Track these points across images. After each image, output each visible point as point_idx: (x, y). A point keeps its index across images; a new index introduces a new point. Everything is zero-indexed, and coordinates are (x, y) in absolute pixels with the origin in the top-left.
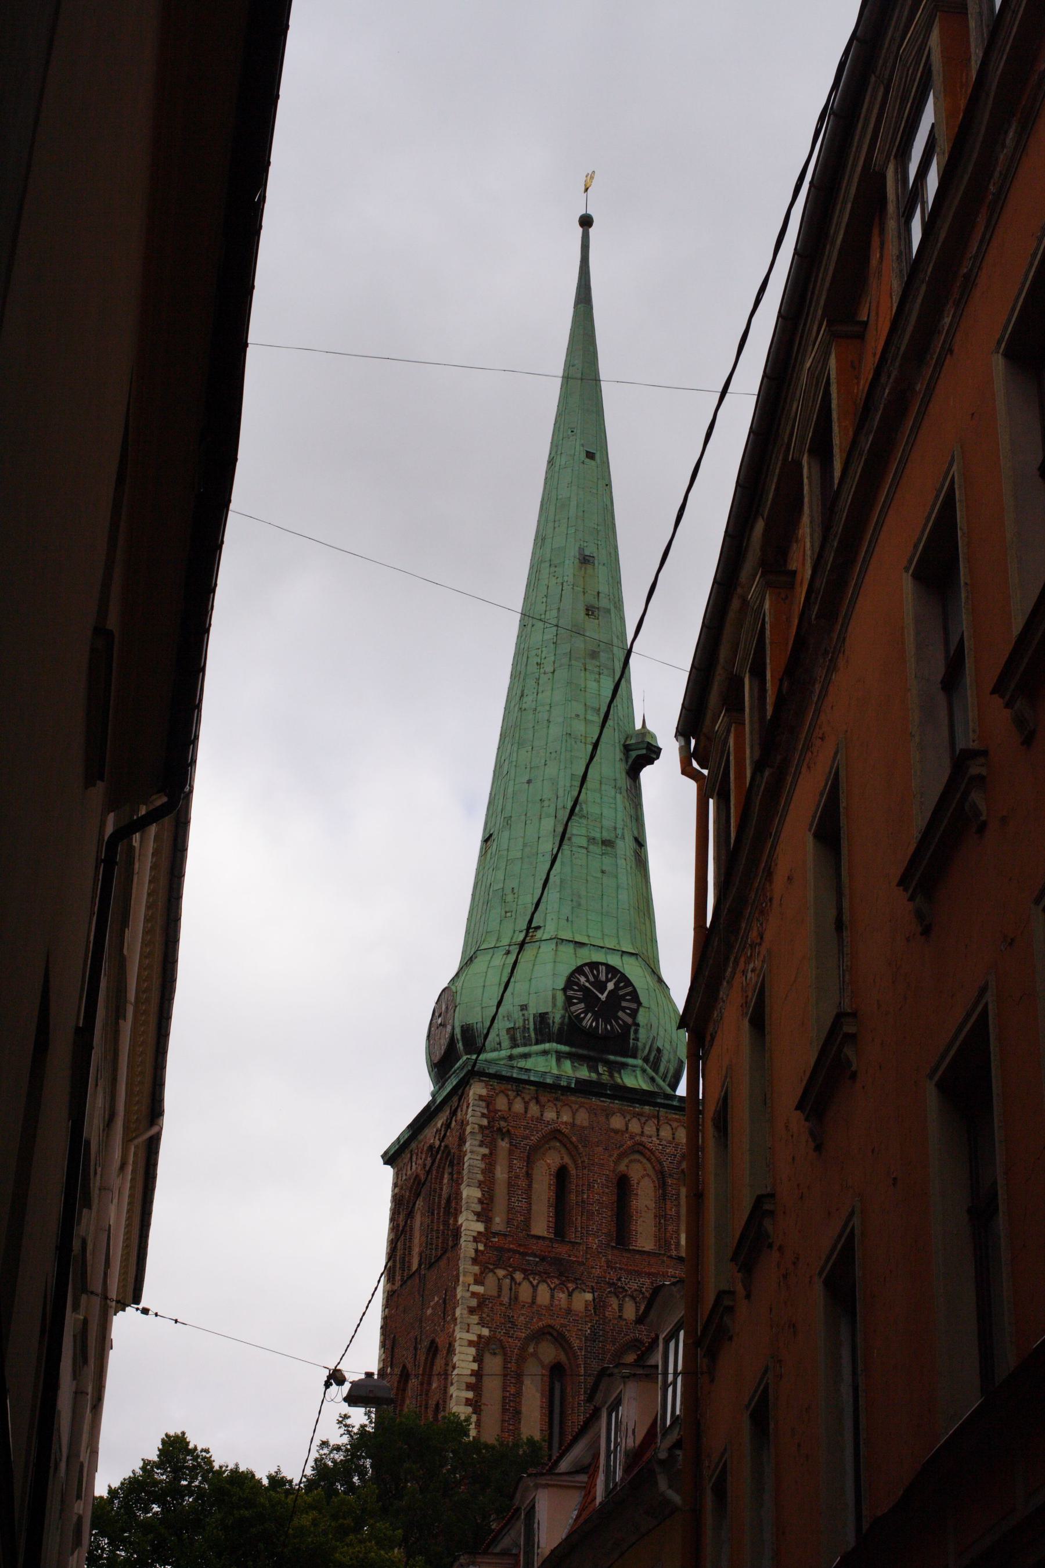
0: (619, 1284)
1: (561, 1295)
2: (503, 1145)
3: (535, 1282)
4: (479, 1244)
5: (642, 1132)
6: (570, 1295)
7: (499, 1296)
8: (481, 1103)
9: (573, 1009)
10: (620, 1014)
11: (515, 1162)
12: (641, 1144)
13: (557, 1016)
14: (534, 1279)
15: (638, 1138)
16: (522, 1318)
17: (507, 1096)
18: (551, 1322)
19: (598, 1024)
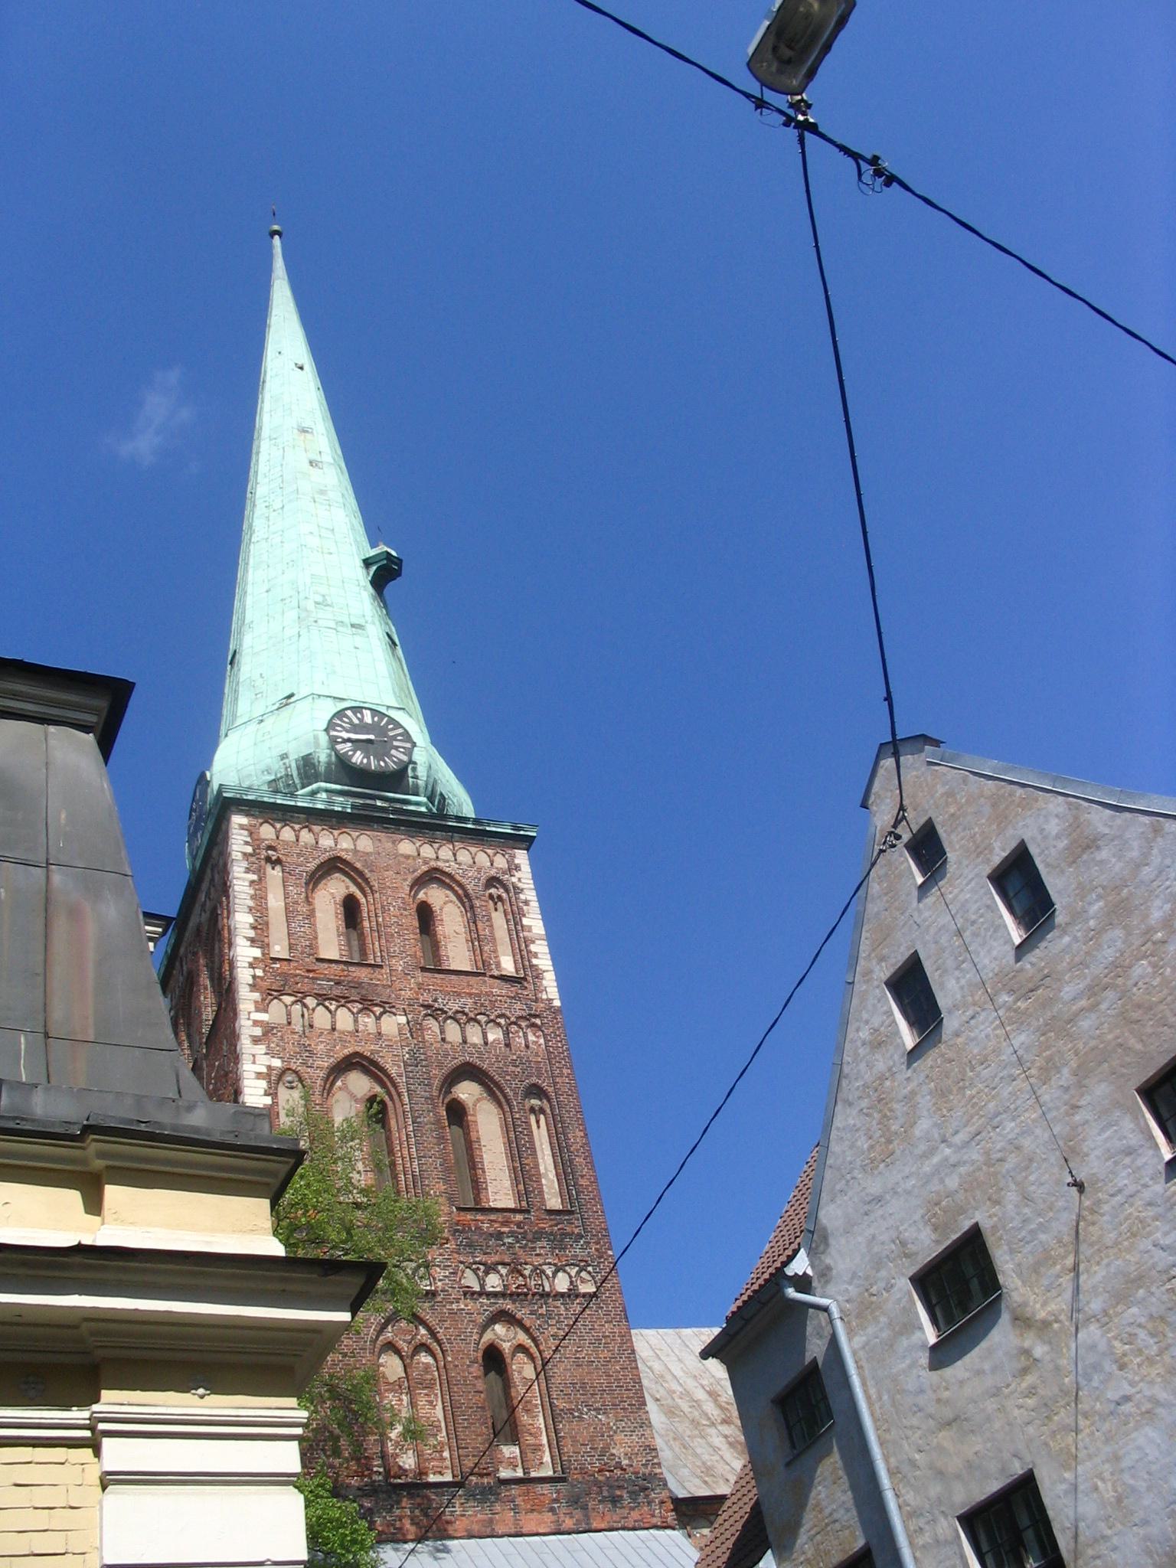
0: (436, 1005)
1: (366, 1020)
2: (275, 874)
3: (333, 1008)
4: (256, 970)
5: (437, 857)
6: (378, 1018)
7: (289, 1023)
8: (242, 831)
9: (338, 747)
10: (393, 752)
11: (291, 888)
12: (436, 869)
13: (323, 756)
14: (331, 1004)
15: (433, 864)
16: (322, 1046)
17: (273, 826)
18: (358, 1049)
19: (369, 759)
